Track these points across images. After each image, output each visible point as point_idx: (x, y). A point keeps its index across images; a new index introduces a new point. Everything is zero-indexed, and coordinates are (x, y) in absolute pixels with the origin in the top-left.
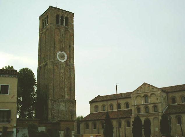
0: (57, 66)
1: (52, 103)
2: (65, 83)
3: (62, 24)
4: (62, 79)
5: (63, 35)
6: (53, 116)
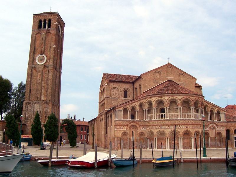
0: (35, 69)
1: (27, 105)
2: (41, 85)
3: (45, 27)
4: (38, 81)
5: (44, 38)
6: (27, 118)
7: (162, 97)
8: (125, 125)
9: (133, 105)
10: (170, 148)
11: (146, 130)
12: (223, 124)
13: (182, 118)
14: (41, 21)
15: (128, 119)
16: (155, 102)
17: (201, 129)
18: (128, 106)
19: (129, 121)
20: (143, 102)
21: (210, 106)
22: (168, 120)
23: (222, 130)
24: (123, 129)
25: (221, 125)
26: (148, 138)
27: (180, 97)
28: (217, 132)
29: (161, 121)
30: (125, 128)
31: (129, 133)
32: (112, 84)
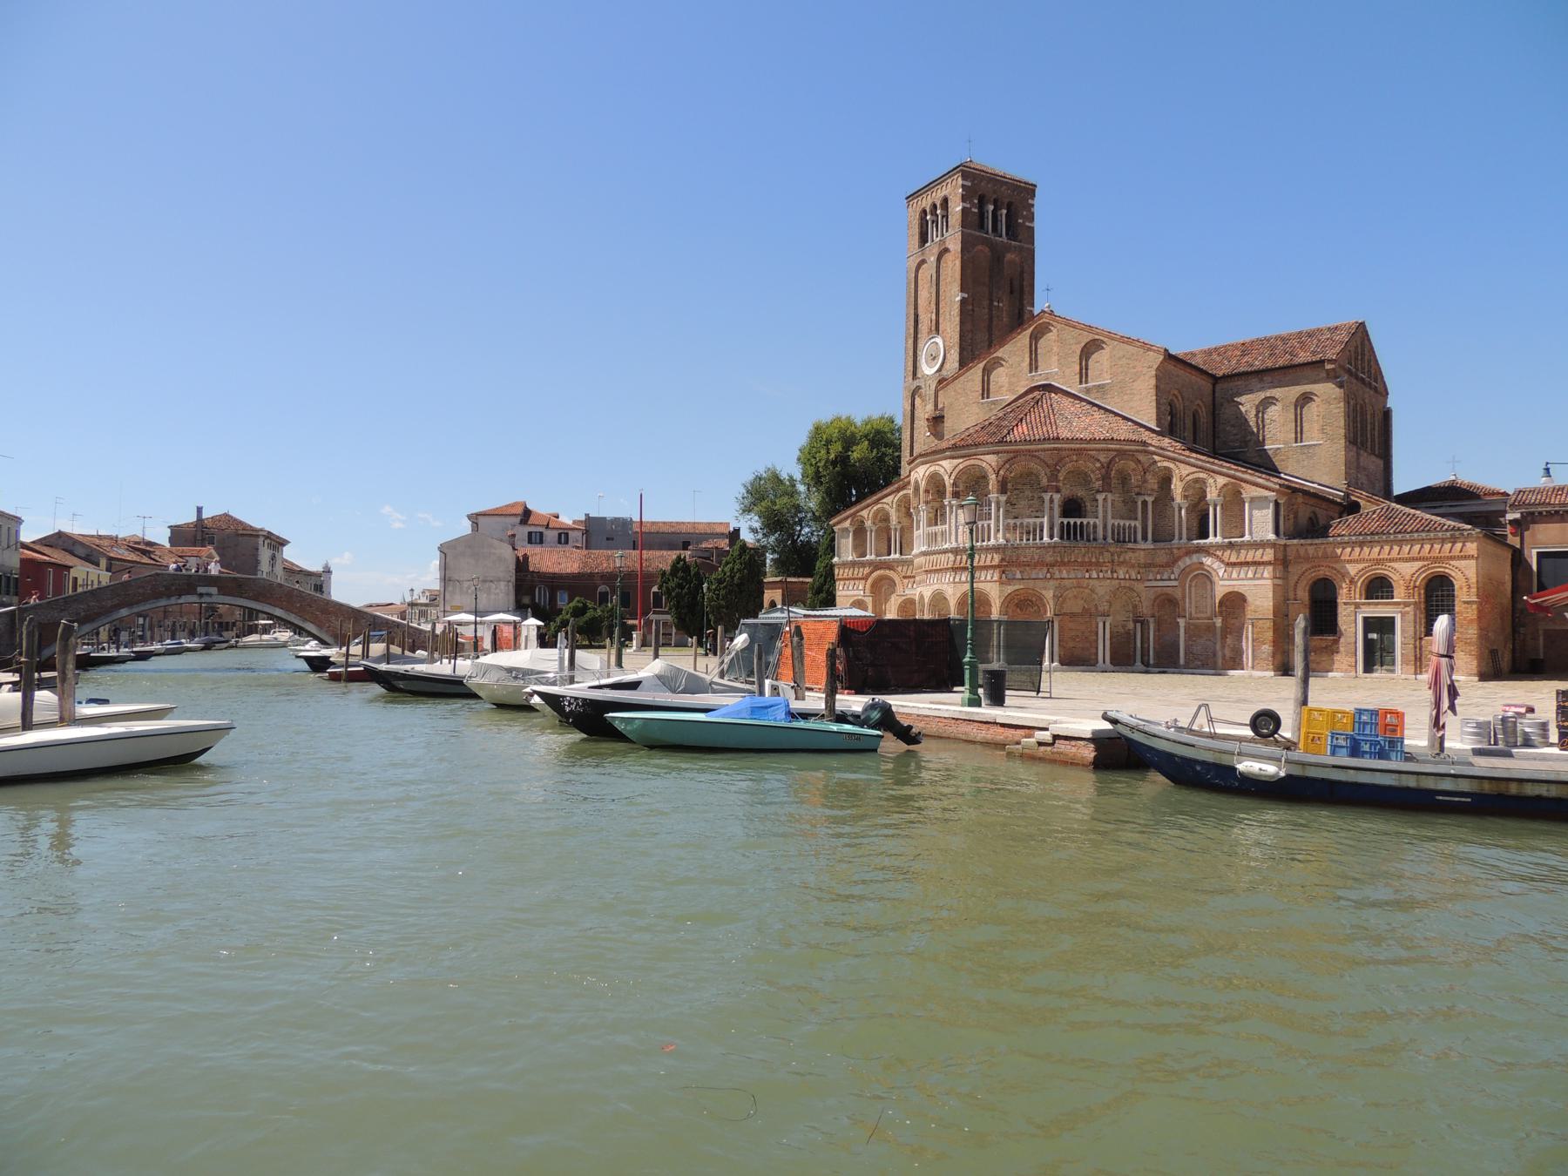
0: (920, 396)
8: (860, 579)
9: (879, 506)
12: (1258, 555)
14: (926, 215)
15: (868, 557)
17: (1052, 583)
18: (864, 513)
19: (870, 563)
23: (1257, 582)
25: (1249, 559)
30: (861, 587)
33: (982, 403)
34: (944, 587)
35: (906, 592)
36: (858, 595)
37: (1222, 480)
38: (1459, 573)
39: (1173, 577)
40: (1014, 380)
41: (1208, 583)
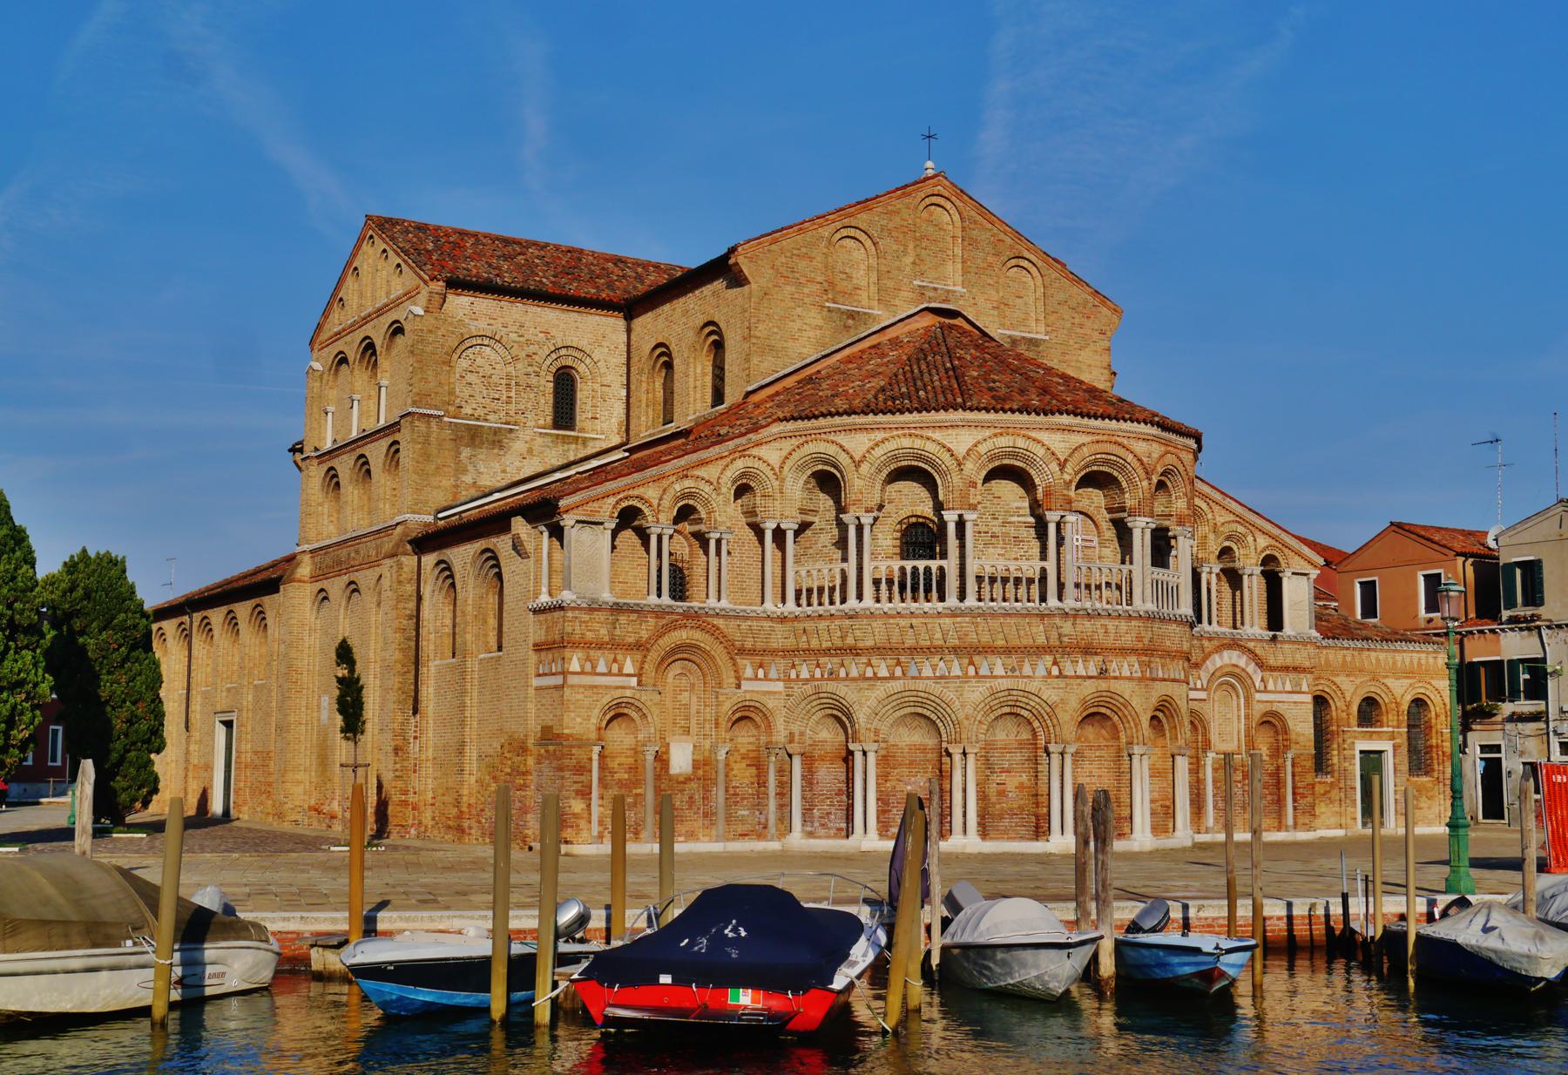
7: (930, 433)
9: (688, 483)
10: (883, 832)
11: (779, 686)
12: (1301, 657)
13: (1069, 603)
15: (653, 599)
16: (865, 468)
18: (651, 493)
19: (659, 613)
20: (763, 466)
21: (1221, 517)
22: (970, 613)
24: (609, 674)
25: (1289, 662)
26: (793, 748)
27: (1060, 443)
28: (1258, 710)
29: (914, 621)
30: (629, 667)
31: (656, 711)
32: (460, 304)
33: (830, 310)
34: (1033, 686)
35: (744, 687)
36: (624, 688)
37: (1263, 542)
38: (1438, 696)
39: (1199, 686)
40: (890, 284)
41: (1235, 697)
